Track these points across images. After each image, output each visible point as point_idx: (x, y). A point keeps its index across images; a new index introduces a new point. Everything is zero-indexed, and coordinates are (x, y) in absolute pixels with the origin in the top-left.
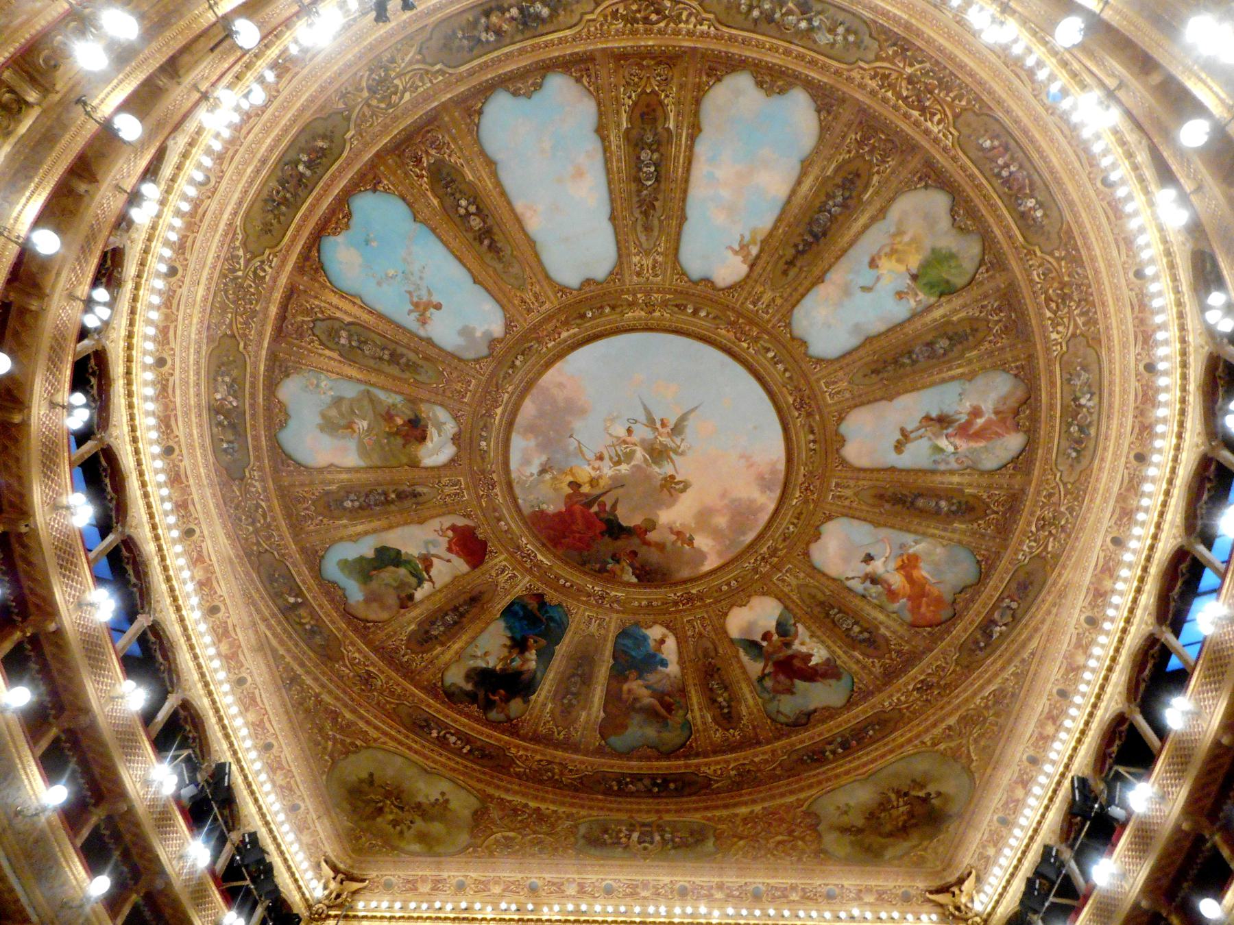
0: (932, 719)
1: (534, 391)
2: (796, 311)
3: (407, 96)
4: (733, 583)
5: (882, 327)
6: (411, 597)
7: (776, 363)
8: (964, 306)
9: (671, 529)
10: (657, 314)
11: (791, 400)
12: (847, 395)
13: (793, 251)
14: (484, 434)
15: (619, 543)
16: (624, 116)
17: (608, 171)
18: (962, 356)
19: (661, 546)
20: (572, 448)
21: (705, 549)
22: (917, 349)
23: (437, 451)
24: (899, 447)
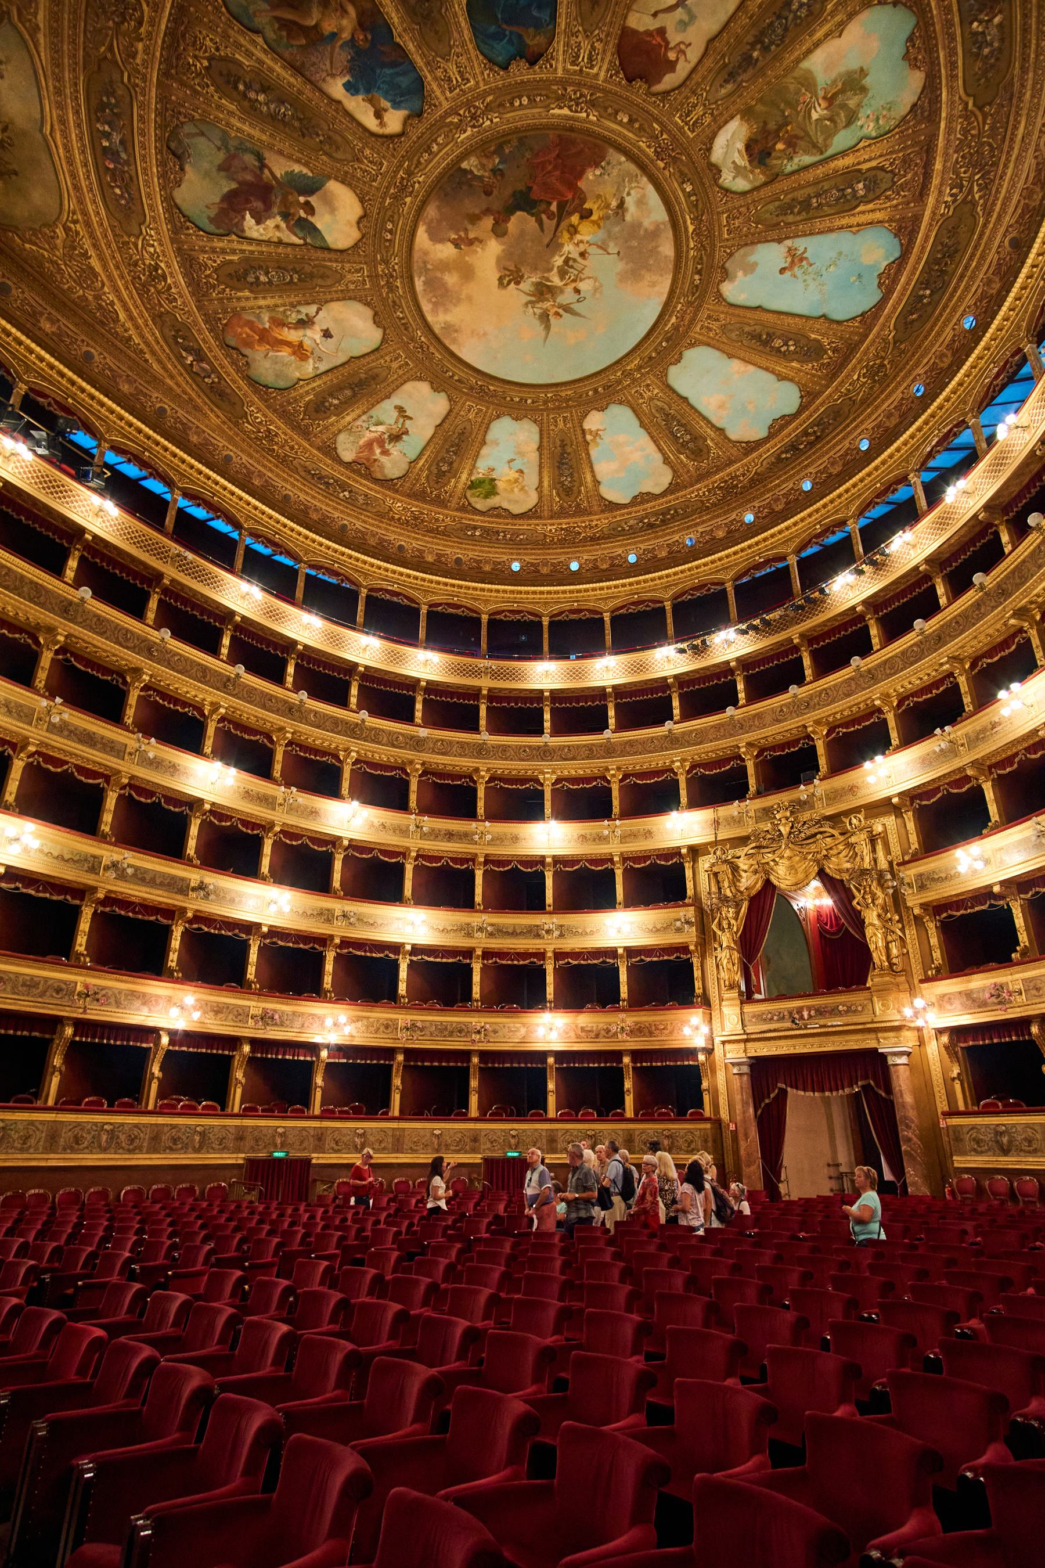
0: (107, 253)
1: (671, 266)
3: (855, 377)
4: (389, 237)
9: (481, 241)
14: (693, 198)
15: (508, 192)
17: (705, 418)
18: (429, 469)
19: (474, 219)
20: (611, 244)
21: (439, 246)
23: (729, 143)
24: (401, 410)
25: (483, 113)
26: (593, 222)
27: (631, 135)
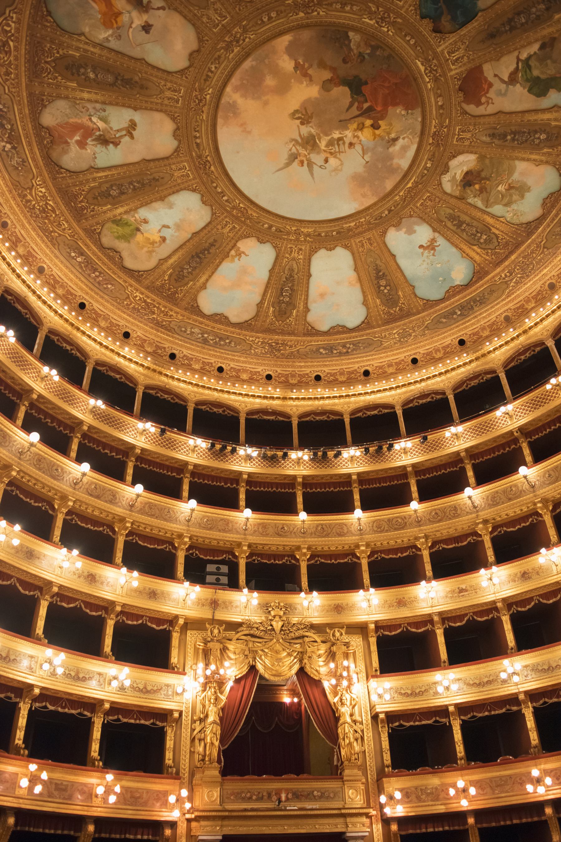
1: (382, 195)
2: (209, 220)
3: (395, 332)
4: (265, 20)
5: (154, 204)
6: (543, 47)
7: (222, 192)
8: (105, 212)
9: (311, 80)
10: (293, 229)
11: (212, 168)
12: (173, 167)
13: (211, 251)
14: (426, 172)
16: (294, 314)
18: (101, 184)
19: (322, 65)
20: (369, 154)
21: (286, 57)
22: (130, 191)
24: (133, 125)
25: (389, 23)
26: (374, 134)
27: (434, 112)
